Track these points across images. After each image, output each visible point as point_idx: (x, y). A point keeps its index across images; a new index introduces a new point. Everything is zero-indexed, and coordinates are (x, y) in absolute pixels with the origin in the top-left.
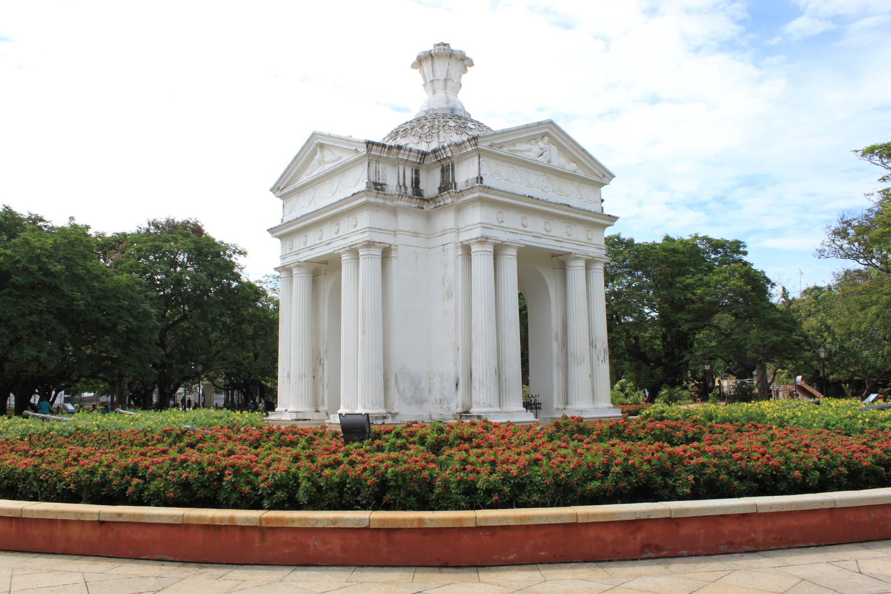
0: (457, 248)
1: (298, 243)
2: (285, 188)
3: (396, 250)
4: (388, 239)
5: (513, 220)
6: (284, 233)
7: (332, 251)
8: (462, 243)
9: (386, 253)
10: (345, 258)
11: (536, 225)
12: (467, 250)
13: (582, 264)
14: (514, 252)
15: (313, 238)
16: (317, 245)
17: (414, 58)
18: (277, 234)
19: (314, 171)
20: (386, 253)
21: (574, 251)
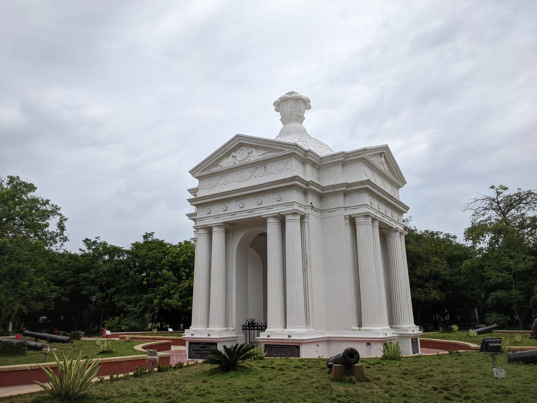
0: (345, 219)
1: (217, 210)
2: (205, 171)
3: (307, 218)
5: (376, 204)
6: (201, 203)
7: (258, 215)
8: (350, 216)
9: (303, 217)
10: (270, 221)
11: (383, 208)
12: (352, 221)
13: (398, 234)
15: (233, 207)
16: (237, 211)
17: (276, 98)
18: (193, 203)
19: (227, 163)
20: (303, 217)
21: (394, 227)
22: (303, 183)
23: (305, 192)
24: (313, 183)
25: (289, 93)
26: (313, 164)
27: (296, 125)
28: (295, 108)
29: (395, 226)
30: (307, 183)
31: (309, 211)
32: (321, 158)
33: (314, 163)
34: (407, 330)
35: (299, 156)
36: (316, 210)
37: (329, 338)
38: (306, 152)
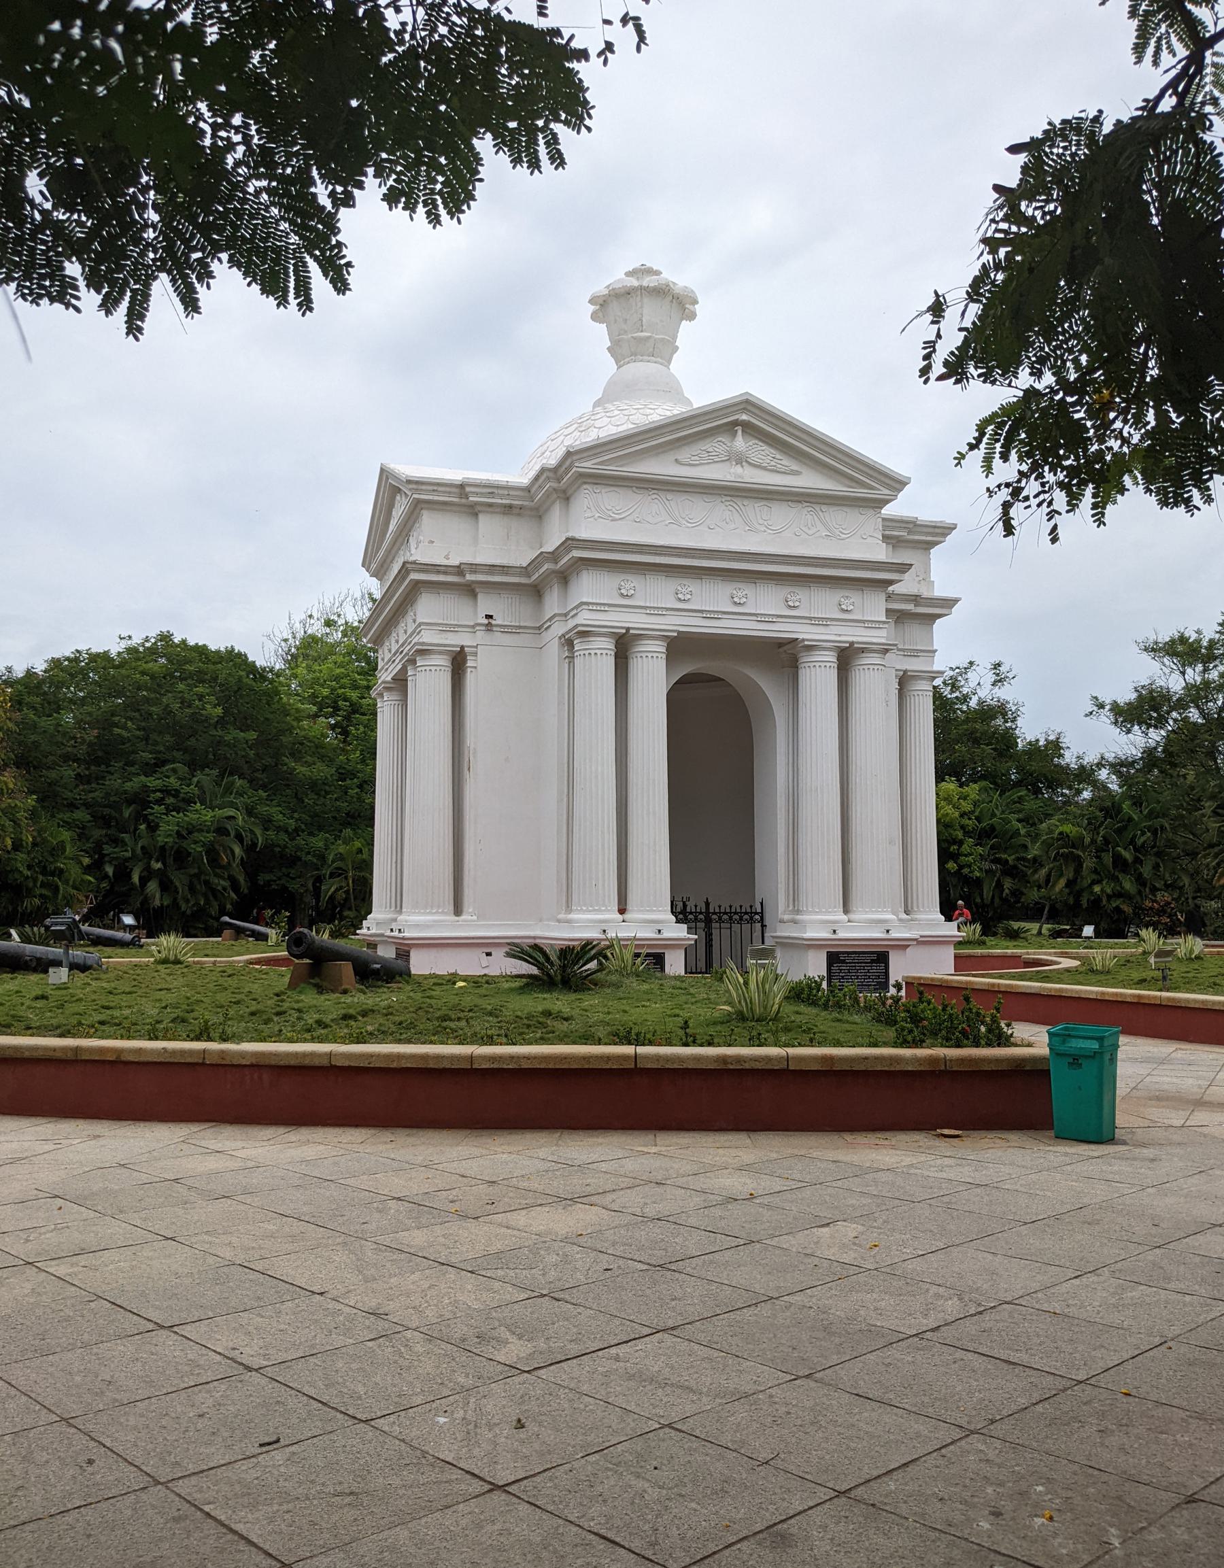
3: (475, 654)
4: (455, 640)
14: (660, 648)
17: (588, 298)
21: (800, 636)
22: (445, 573)
23: (470, 591)
24: (475, 568)
25: (628, 274)
26: (508, 510)
27: (641, 369)
28: (625, 321)
29: (805, 633)
30: (459, 570)
31: (481, 636)
32: (527, 489)
33: (511, 507)
34: (804, 930)
35: (445, 503)
36: (508, 630)
37: (534, 938)
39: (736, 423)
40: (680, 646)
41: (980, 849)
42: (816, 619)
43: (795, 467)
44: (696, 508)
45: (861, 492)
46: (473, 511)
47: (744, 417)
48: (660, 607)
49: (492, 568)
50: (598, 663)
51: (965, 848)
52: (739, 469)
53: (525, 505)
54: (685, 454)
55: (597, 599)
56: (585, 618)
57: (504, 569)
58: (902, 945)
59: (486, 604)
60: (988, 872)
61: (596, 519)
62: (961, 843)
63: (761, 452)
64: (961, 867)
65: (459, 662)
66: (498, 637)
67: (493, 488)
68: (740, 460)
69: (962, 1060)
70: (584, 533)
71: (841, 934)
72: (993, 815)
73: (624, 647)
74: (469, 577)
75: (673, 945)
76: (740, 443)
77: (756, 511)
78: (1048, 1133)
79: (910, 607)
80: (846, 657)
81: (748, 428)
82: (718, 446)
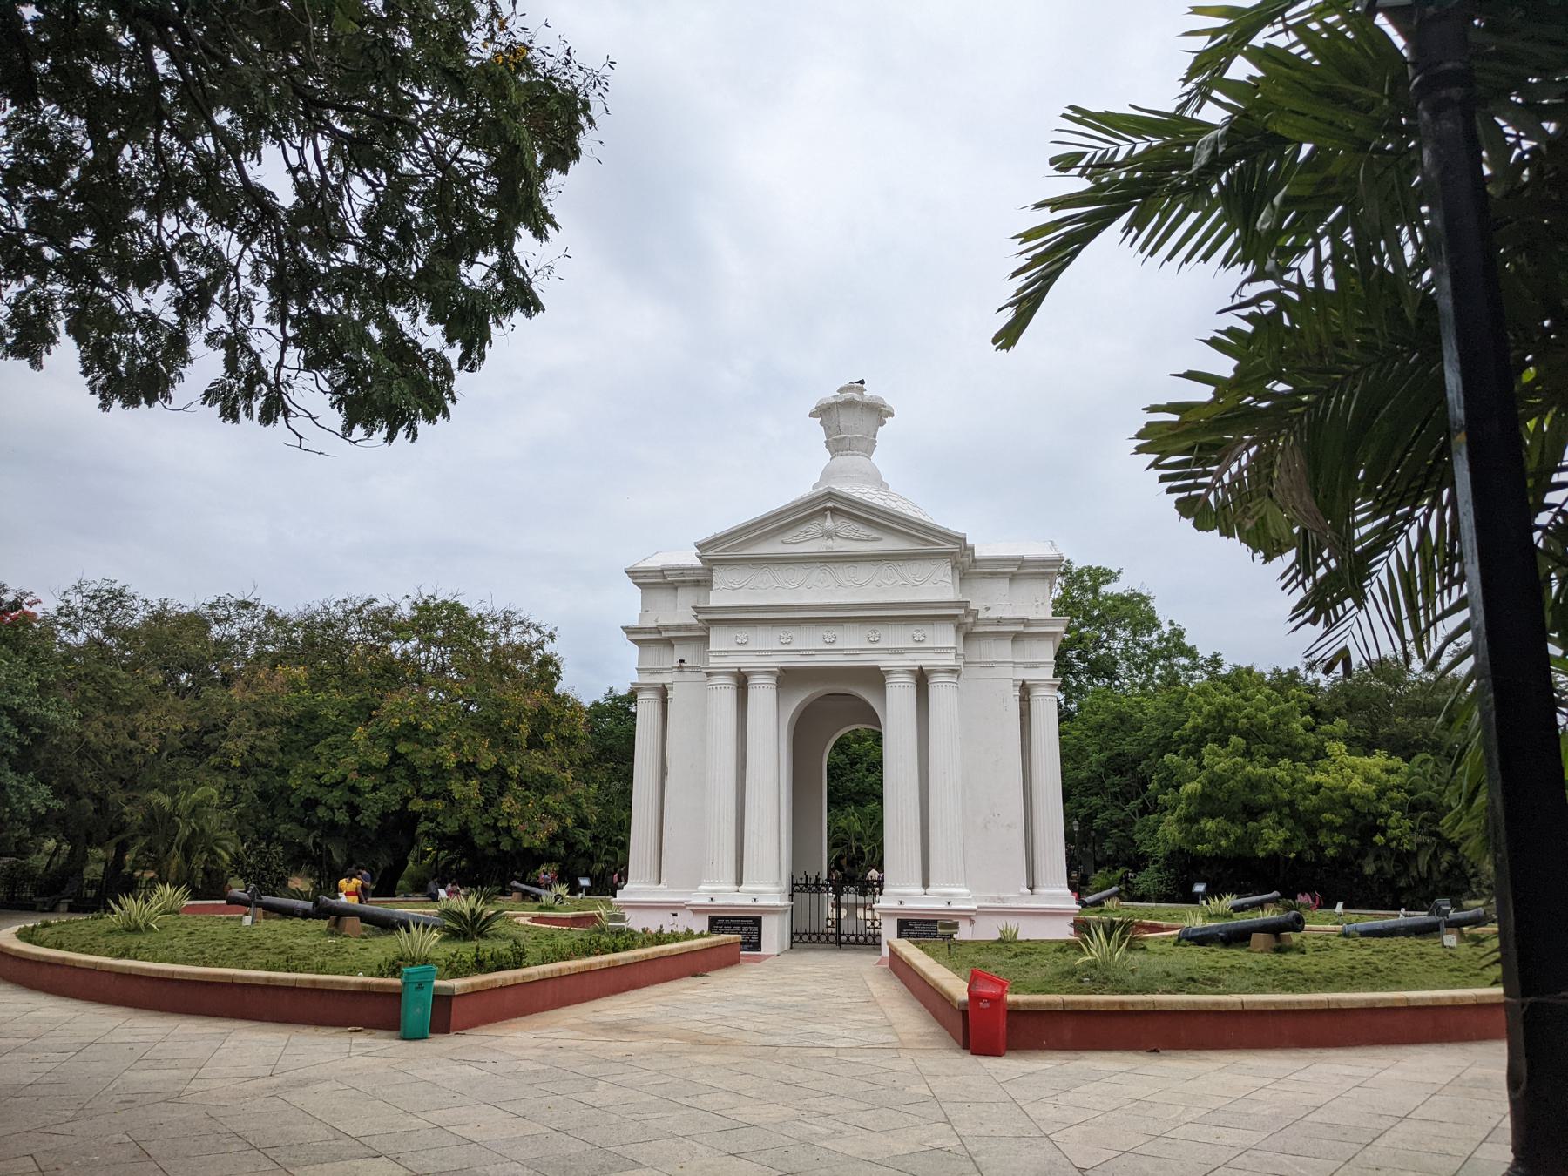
4: (659, 680)
23: (669, 643)
24: (667, 628)
25: (841, 390)
26: (697, 583)
27: (845, 460)
29: (884, 661)
30: (658, 630)
31: (676, 676)
38: (662, 571)
39: (826, 509)
40: (787, 678)
41: (1409, 823)
42: (894, 651)
43: (875, 535)
44: (797, 574)
45: (936, 549)
46: (674, 586)
47: (829, 504)
48: (766, 650)
49: (679, 627)
50: (725, 696)
51: (1392, 822)
52: (830, 542)
53: (700, 581)
54: (788, 537)
55: (726, 648)
56: (714, 662)
57: (687, 627)
58: (969, 917)
59: (680, 652)
60: (1420, 846)
61: (728, 591)
62: (1389, 815)
63: (848, 527)
64: (1389, 841)
65: (663, 693)
66: (688, 676)
67: (682, 570)
68: (829, 535)
69: (379, 985)
70: (713, 603)
71: (906, 905)
72: (1430, 788)
73: (742, 681)
74: (664, 635)
75: (772, 911)
76: (829, 523)
77: (845, 573)
78: (394, 1033)
79: (1020, 628)
80: (922, 679)
81: (834, 511)
82: (813, 528)
